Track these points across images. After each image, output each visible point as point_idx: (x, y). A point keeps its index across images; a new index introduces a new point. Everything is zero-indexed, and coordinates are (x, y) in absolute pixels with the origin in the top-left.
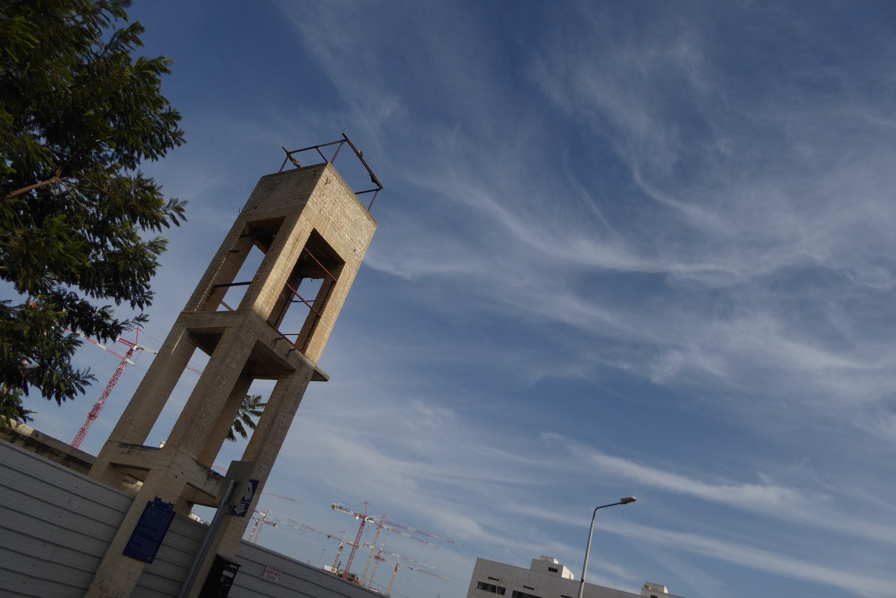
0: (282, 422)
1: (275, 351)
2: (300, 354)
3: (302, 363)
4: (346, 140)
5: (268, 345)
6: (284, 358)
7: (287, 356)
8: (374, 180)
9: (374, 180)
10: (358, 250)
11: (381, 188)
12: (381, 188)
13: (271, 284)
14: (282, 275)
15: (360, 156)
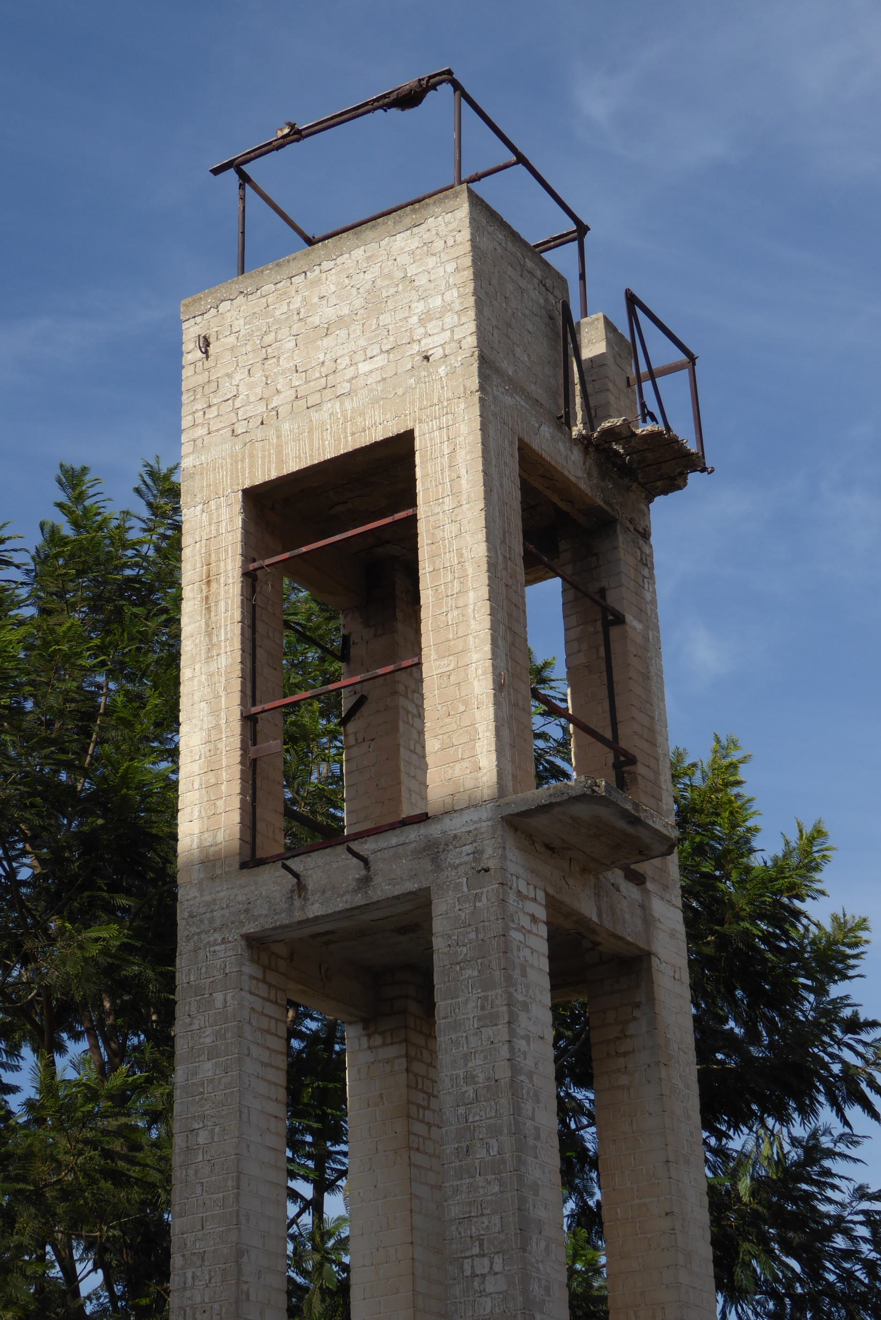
0: (470, 1078)
1: (315, 909)
2: (413, 834)
3: (433, 851)
4: (236, 165)
5: (283, 919)
6: (359, 900)
7: (365, 881)
8: (409, 99)
9: (409, 99)
10: (434, 343)
11: (448, 76)
12: (448, 76)
13: (196, 768)
14: (215, 713)
15: (297, 135)
